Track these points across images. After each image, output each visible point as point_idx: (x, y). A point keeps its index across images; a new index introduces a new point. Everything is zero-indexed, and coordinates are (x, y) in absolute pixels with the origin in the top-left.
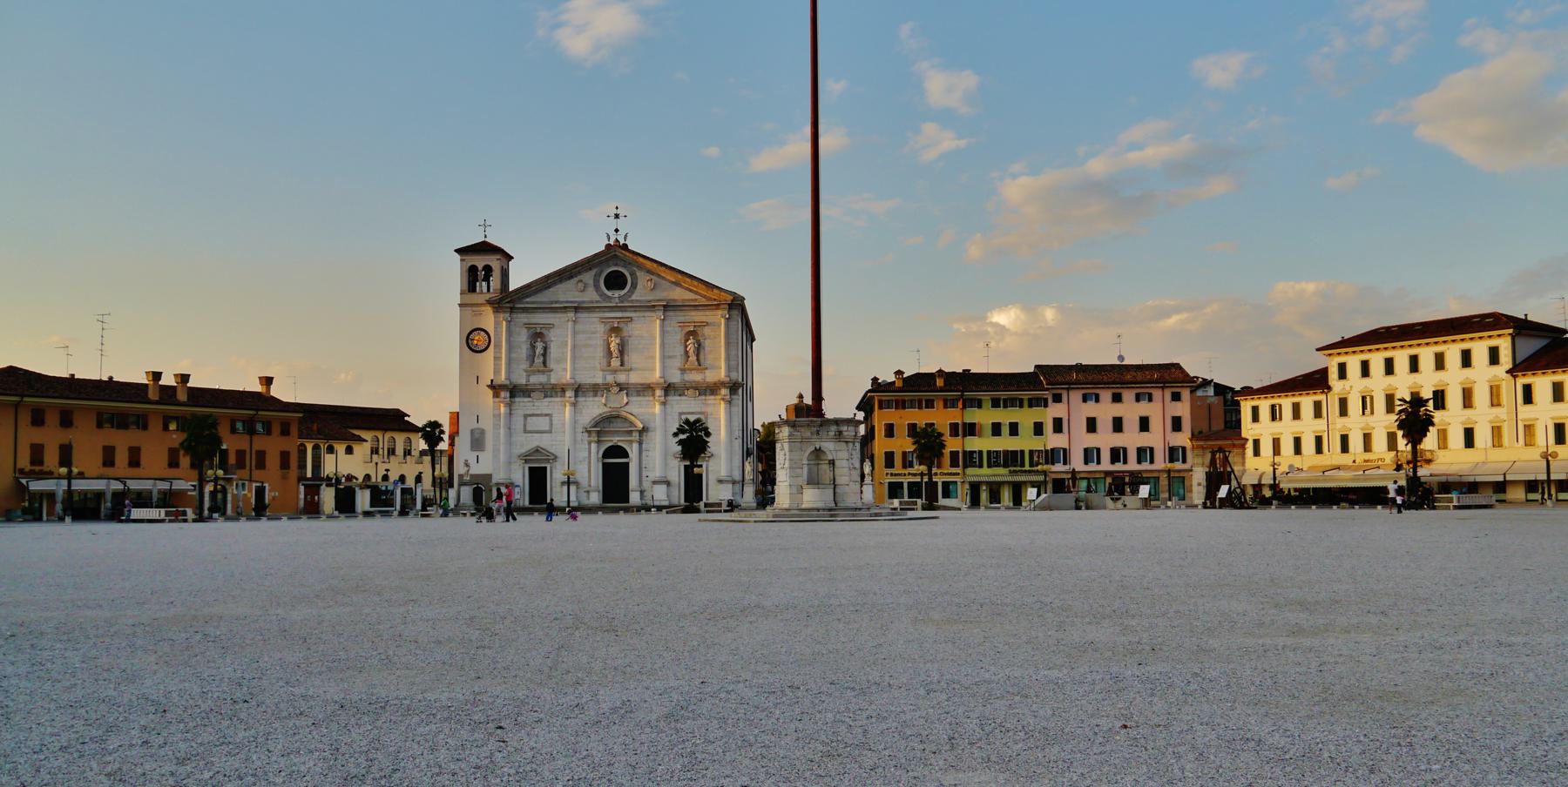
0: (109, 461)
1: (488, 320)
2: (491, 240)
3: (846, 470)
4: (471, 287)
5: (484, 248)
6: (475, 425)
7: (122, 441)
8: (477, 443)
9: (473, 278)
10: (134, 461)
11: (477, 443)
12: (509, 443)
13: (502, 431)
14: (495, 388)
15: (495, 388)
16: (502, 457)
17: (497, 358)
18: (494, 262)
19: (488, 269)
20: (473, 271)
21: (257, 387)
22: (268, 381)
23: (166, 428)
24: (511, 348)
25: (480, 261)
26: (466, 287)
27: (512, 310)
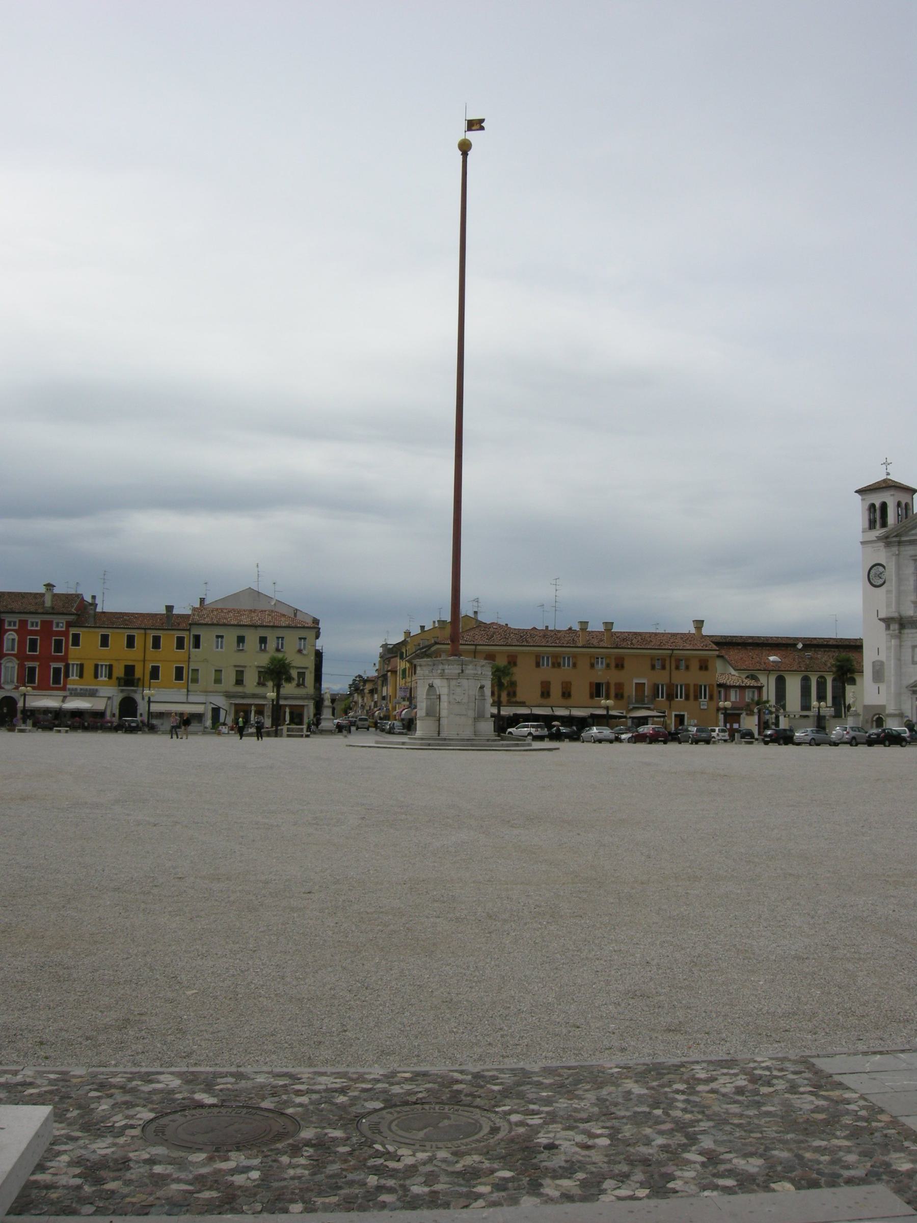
0: (546, 694)
1: (881, 555)
2: (896, 477)
3: (446, 704)
4: (872, 525)
5: (887, 485)
6: (877, 658)
7: (556, 677)
8: (878, 676)
9: (877, 516)
10: (566, 694)
11: (878, 676)
12: (899, 674)
13: (892, 662)
14: (888, 621)
15: (888, 621)
16: (892, 689)
17: (889, 592)
18: (890, 499)
19: (884, 506)
20: (873, 506)
21: (693, 631)
22: (699, 624)
23: (592, 666)
24: (900, 580)
25: (877, 499)
26: (867, 525)
27: (900, 543)
